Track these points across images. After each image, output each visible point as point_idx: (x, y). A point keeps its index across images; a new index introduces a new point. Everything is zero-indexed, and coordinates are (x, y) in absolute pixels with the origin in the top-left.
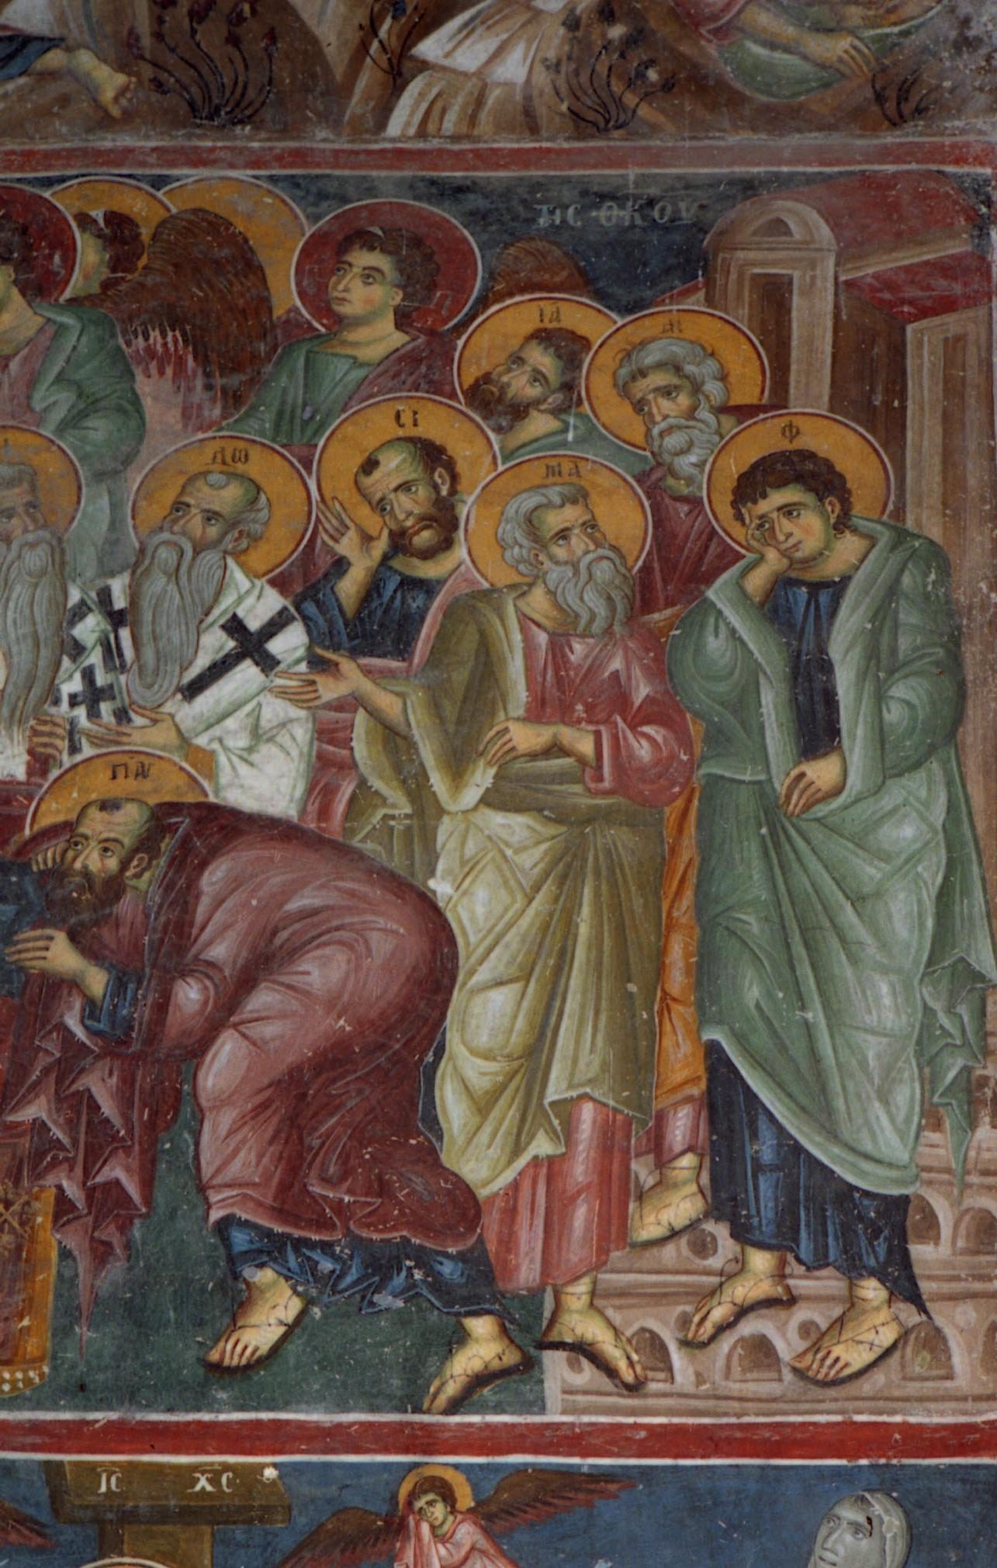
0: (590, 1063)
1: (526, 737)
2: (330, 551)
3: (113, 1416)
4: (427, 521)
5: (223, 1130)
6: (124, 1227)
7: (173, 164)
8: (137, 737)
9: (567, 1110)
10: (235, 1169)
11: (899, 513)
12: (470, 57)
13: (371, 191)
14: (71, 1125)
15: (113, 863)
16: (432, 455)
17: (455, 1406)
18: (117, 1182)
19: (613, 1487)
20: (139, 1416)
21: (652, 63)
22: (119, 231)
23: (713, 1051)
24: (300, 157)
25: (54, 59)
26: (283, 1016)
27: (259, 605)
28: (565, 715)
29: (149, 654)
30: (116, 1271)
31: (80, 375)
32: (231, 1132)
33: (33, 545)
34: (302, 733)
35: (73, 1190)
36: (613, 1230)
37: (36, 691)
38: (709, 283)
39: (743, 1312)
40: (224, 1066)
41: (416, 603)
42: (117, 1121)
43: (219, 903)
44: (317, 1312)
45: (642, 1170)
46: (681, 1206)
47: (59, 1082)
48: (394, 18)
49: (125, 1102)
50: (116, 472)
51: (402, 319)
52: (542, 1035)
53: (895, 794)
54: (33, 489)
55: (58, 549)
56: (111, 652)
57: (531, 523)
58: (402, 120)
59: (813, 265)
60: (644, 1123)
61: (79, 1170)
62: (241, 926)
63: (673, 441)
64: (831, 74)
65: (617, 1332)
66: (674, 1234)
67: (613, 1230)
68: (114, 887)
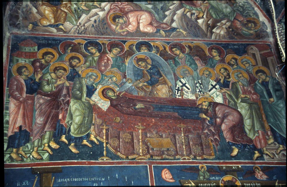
0: (259, 127)
1: (243, 96)
2: (219, 78)
3: (223, 161)
4: (227, 75)
5: (225, 133)
6: (218, 142)
7: (193, 41)
8: (205, 95)
9: (258, 131)
10: (228, 137)
11: (272, 75)
12: (218, 31)
13: (212, 44)
14: (210, 133)
15: (207, 107)
16: (226, 69)
17: (256, 160)
18: (216, 138)
19: (274, 168)
20: (225, 161)
21: (235, 33)
22: (189, 47)
23: (270, 126)
24: (204, 41)
25: (178, 30)
26: (228, 122)
27: (214, 83)
28: (246, 94)
29: (204, 88)
30: (219, 147)
31: (190, 61)
32: (226, 133)
33: (190, 77)
34: (221, 95)
35: (212, 139)
36: (266, 143)
37: (194, 91)
38: (247, 54)
39: (281, 151)
40: (223, 127)
41: (228, 83)
42: (215, 132)
43: (218, 111)
44: (240, 151)
45: (267, 137)
46: (272, 141)
47: (208, 128)
48: (210, 27)
49: (215, 130)
50: (196, 70)
51: (219, 56)
52: (253, 124)
53: (279, 102)
54: (189, 72)
55: (193, 77)
56: (201, 87)
57: (237, 75)
58: (213, 37)
59: (257, 52)
60: (265, 132)
61: (212, 137)
62: (221, 113)
63: (248, 68)
64: (251, 34)
65: (270, 153)
66: (272, 143)
67: (266, 143)
68: (207, 110)
